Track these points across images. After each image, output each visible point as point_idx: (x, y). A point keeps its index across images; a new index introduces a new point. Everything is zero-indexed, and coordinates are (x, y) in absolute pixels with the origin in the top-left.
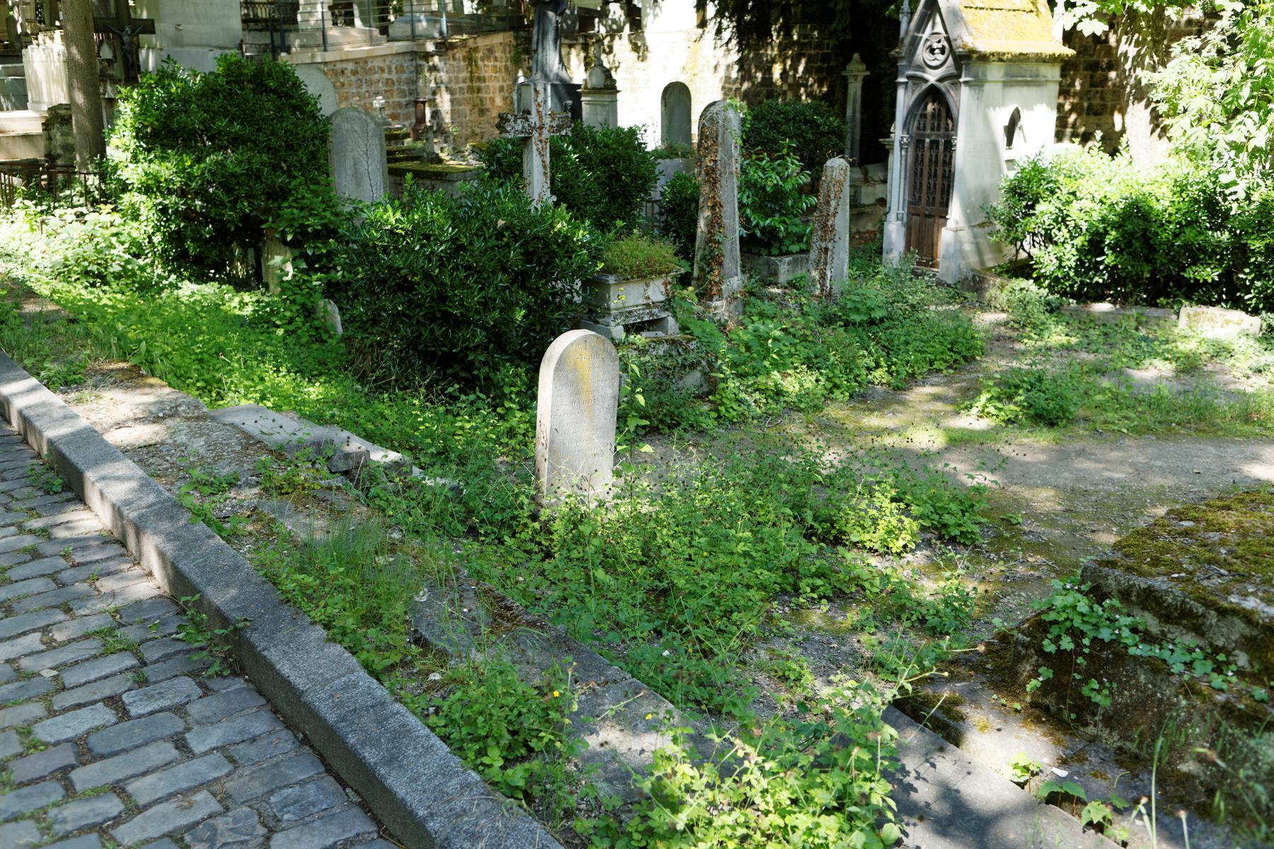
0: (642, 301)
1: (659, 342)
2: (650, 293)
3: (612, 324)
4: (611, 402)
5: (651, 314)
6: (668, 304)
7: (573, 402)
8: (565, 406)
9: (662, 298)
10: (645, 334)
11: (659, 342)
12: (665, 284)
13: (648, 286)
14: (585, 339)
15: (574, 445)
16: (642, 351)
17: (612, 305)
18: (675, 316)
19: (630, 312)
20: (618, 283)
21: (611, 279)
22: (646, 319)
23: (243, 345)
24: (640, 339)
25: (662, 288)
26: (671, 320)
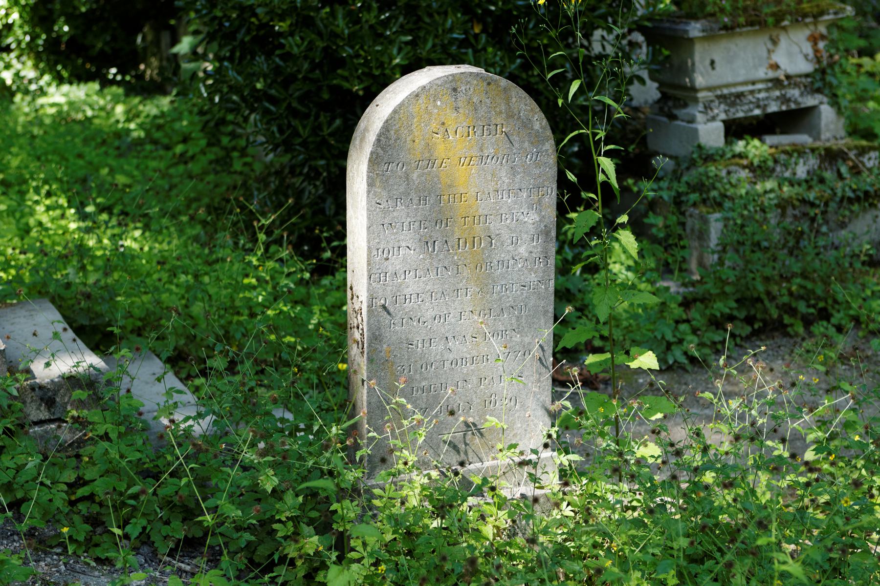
0: (762, 73)
1: (799, 151)
2: (780, 57)
3: (700, 117)
4: (537, 247)
5: (785, 100)
6: (820, 80)
7: (426, 243)
8: (406, 254)
9: (805, 67)
10: (770, 139)
11: (799, 151)
12: (814, 39)
13: (775, 42)
14: (453, 86)
15: (438, 348)
16: (760, 170)
17: (700, 80)
18: (834, 102)
19: (740, 95)
20: (710, 37)
21: (695, 29)
22: (773, 108)
23: (165, 231)
24: (755, 148)
25: (808, 48)
26: (827, 112)
